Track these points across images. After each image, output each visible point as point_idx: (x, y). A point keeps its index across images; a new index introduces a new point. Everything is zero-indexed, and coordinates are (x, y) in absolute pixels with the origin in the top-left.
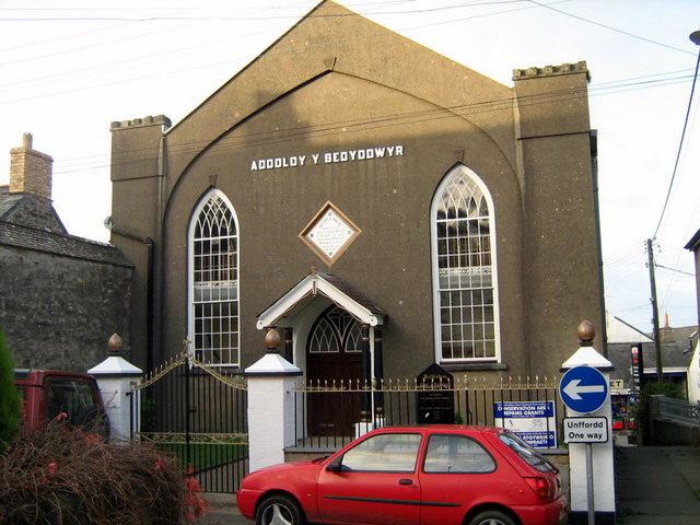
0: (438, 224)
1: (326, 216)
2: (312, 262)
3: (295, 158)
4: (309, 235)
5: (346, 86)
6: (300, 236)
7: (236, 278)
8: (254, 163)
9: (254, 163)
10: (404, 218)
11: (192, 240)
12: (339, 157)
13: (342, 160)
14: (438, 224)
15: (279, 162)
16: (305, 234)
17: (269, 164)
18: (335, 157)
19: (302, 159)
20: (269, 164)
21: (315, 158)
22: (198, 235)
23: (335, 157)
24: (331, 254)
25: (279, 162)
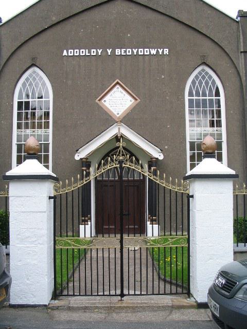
0: (189, 99)
1: (115, 89)
2: (108, 120)
3: (130, 50)
4: (103, 101)
5: (131, 8)
6: (97, 101)
7: (48, 127)
8: (65, 51)
9: (65, 51)
10: (169, 94)
11: (187, 98)
12: (125, 51)
13: (128, 54)
14: (189, 99)
15: (84, 52)
16: (99, 100)
17: (77, 52)
18: (123, 52)
19: (100, 51)
20: (77, 52)
21: (109, 51)
22: (191, 94)
23: (123, 52)
24: (118, 114)
25: (84, 52)
